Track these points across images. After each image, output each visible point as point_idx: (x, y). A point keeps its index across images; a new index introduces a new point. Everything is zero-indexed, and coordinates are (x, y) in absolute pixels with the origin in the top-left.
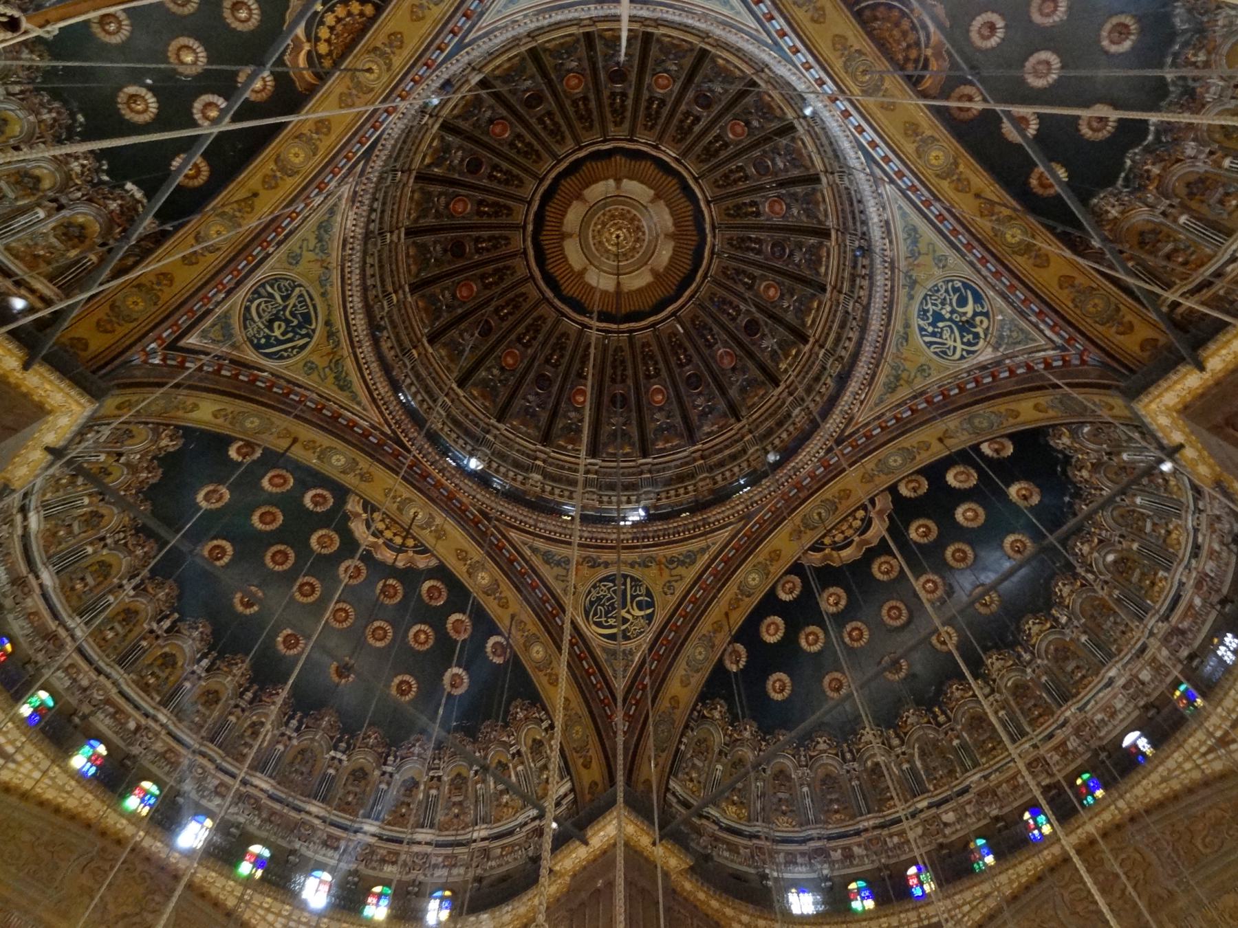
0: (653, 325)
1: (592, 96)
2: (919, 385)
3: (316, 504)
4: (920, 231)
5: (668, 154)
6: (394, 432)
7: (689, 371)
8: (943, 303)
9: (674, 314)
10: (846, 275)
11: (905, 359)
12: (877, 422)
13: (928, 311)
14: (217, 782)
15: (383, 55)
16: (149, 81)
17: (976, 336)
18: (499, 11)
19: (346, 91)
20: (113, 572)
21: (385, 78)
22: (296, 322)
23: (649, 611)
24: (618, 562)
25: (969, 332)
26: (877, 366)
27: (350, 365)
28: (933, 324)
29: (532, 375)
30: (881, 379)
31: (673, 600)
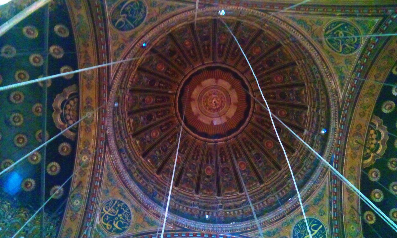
2: (103, 187)
4: (150, 226)
5: (221, 142)
7: (156, 84)
8: (124, 217)
9: (176, 94)
10: (143, 171)
11: (115, 188)
12: (102, 161)
13: (125, 209)
15: (355, 149)
17: (106, 222)
18: (326, 183)
19: (361, 130)
21: (350, 143)
24: (142, 29)
25: (109, 220)
28: (119, 208)
30: (114, 173)
31: (110, 36)
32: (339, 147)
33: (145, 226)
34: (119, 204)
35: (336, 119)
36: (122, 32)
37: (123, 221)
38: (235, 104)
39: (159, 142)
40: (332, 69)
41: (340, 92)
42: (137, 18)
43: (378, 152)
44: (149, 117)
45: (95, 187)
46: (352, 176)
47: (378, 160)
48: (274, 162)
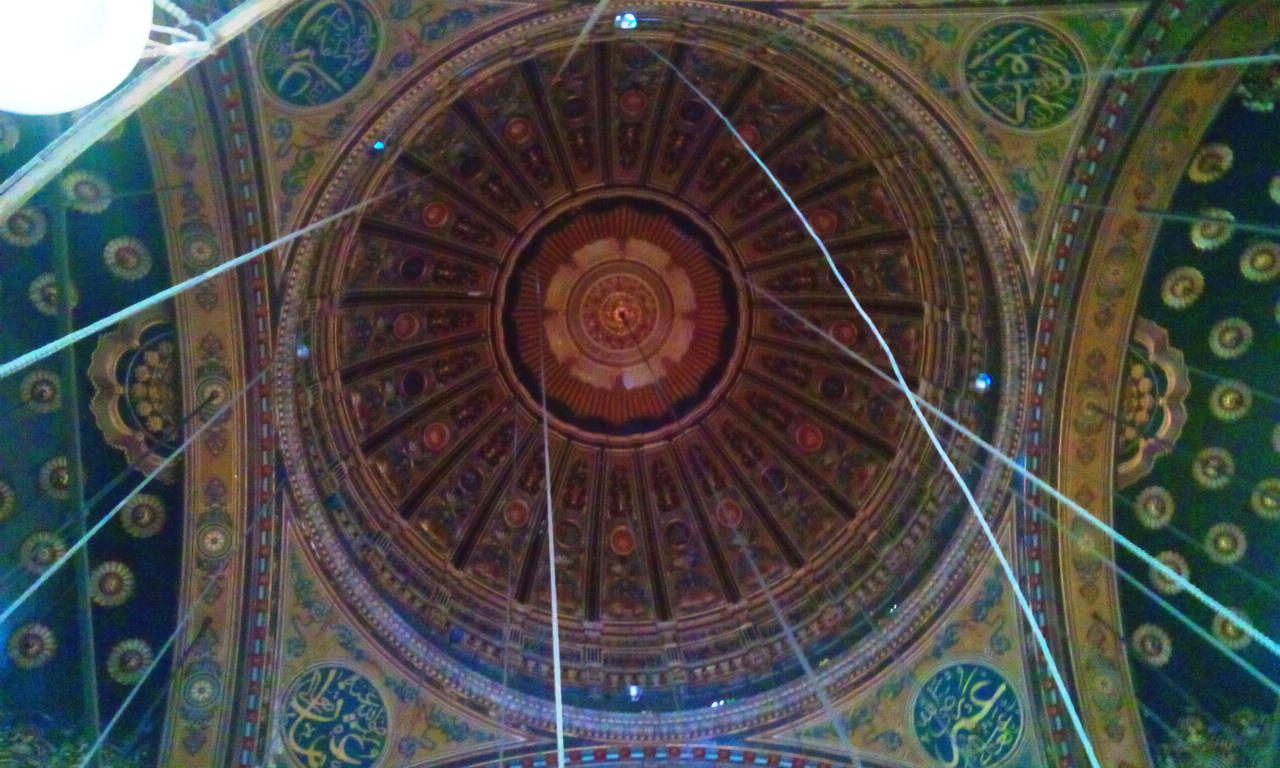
2: (286, 631)
4: (453, 744)
5: (652, 442)
6: (781, 15)
8: (363, 723)
9: (494, 301)
12: (273, 543)
13: (364, 697)
15: (1090, 431)
17: (305, 743)
23: (282, 83)
26: (337, 588)
27: (893, 61)
28: (344, 694)
29: (594, 103)
32: (1039, 430)
33: (434, 744)
34: (343, 678)
35: (1020, 339)
36: (309, 110)
37: (360, 734)
38: (688, 316)
39: (454, 457)
40: (997, 179)
41: (1027, 253)
42: (350, 59)
43: (1163, 432)
44: (414, 384)
45: (259, 633)
47: (1162, 461)
48: (831, 495)
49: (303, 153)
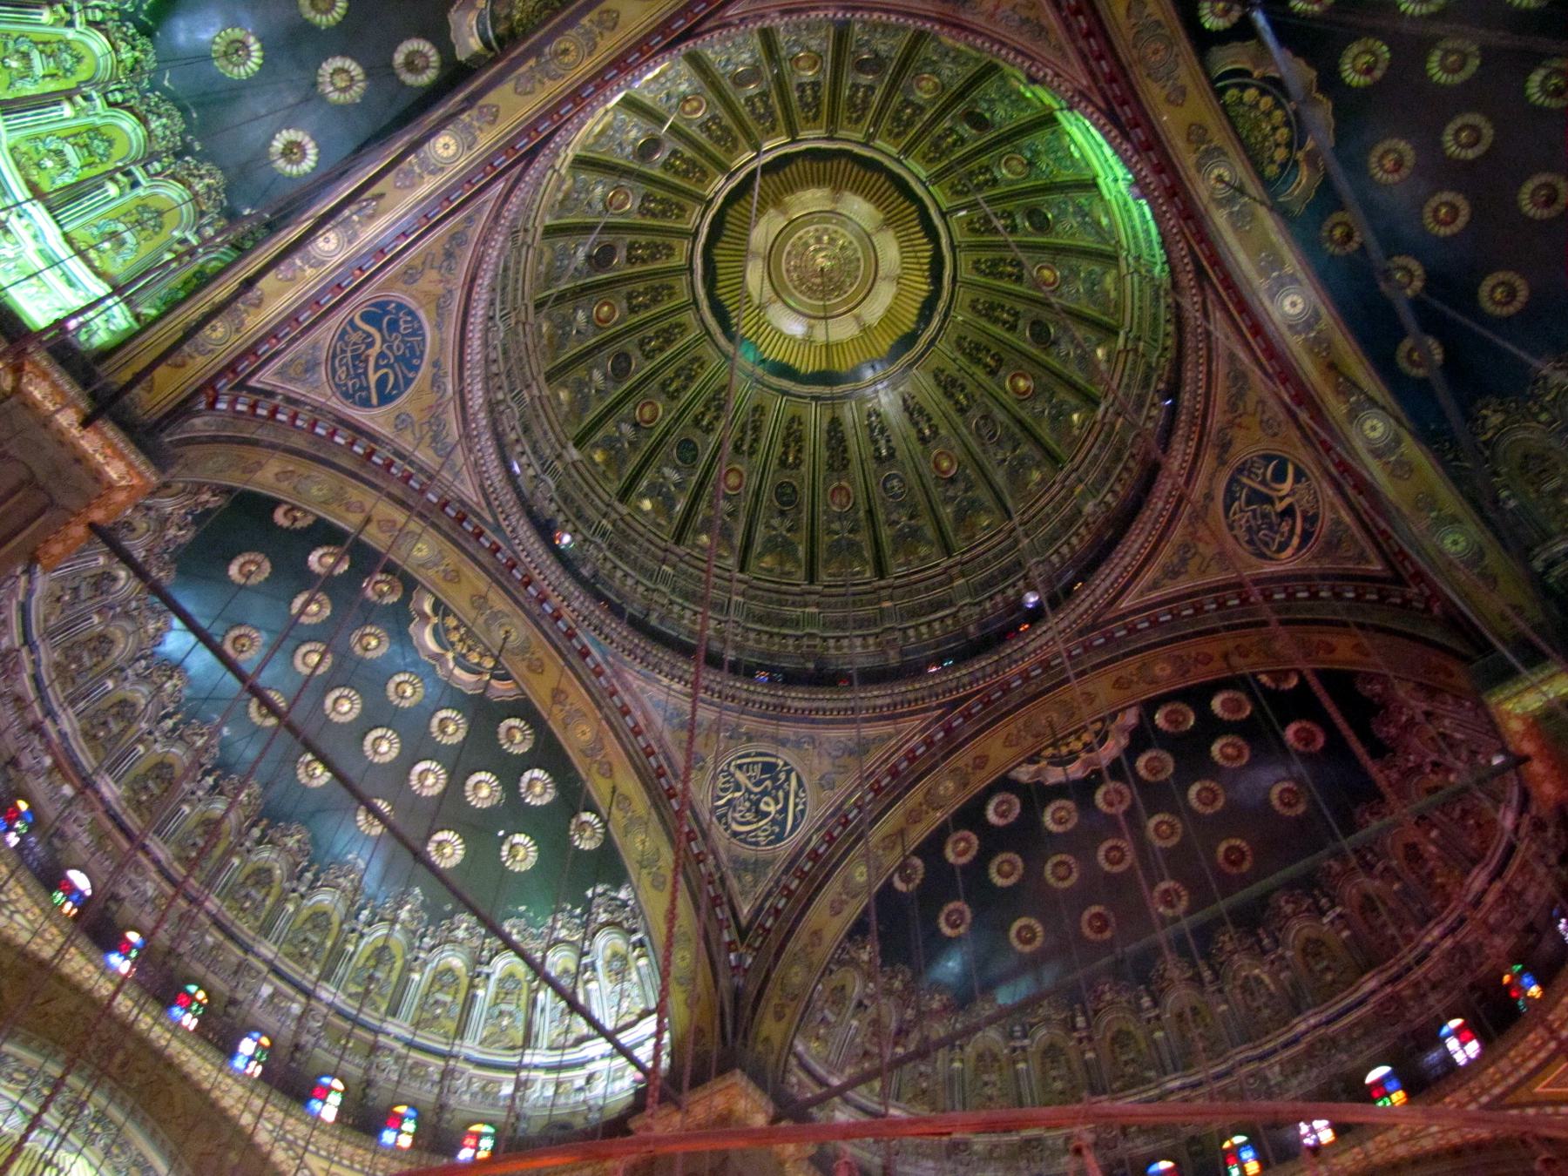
0: (953, 248)
1: (625, 290)
3: (1002, 815)
5: (719, 186)
6: (939, 706)
9: (943, 215)
11: (997, 7)
14: (1277, 1069)
16: (501, 833)
20: (996, 1049)
22: (768, 783)
46: (436, 565)
49: (1241, 410)
